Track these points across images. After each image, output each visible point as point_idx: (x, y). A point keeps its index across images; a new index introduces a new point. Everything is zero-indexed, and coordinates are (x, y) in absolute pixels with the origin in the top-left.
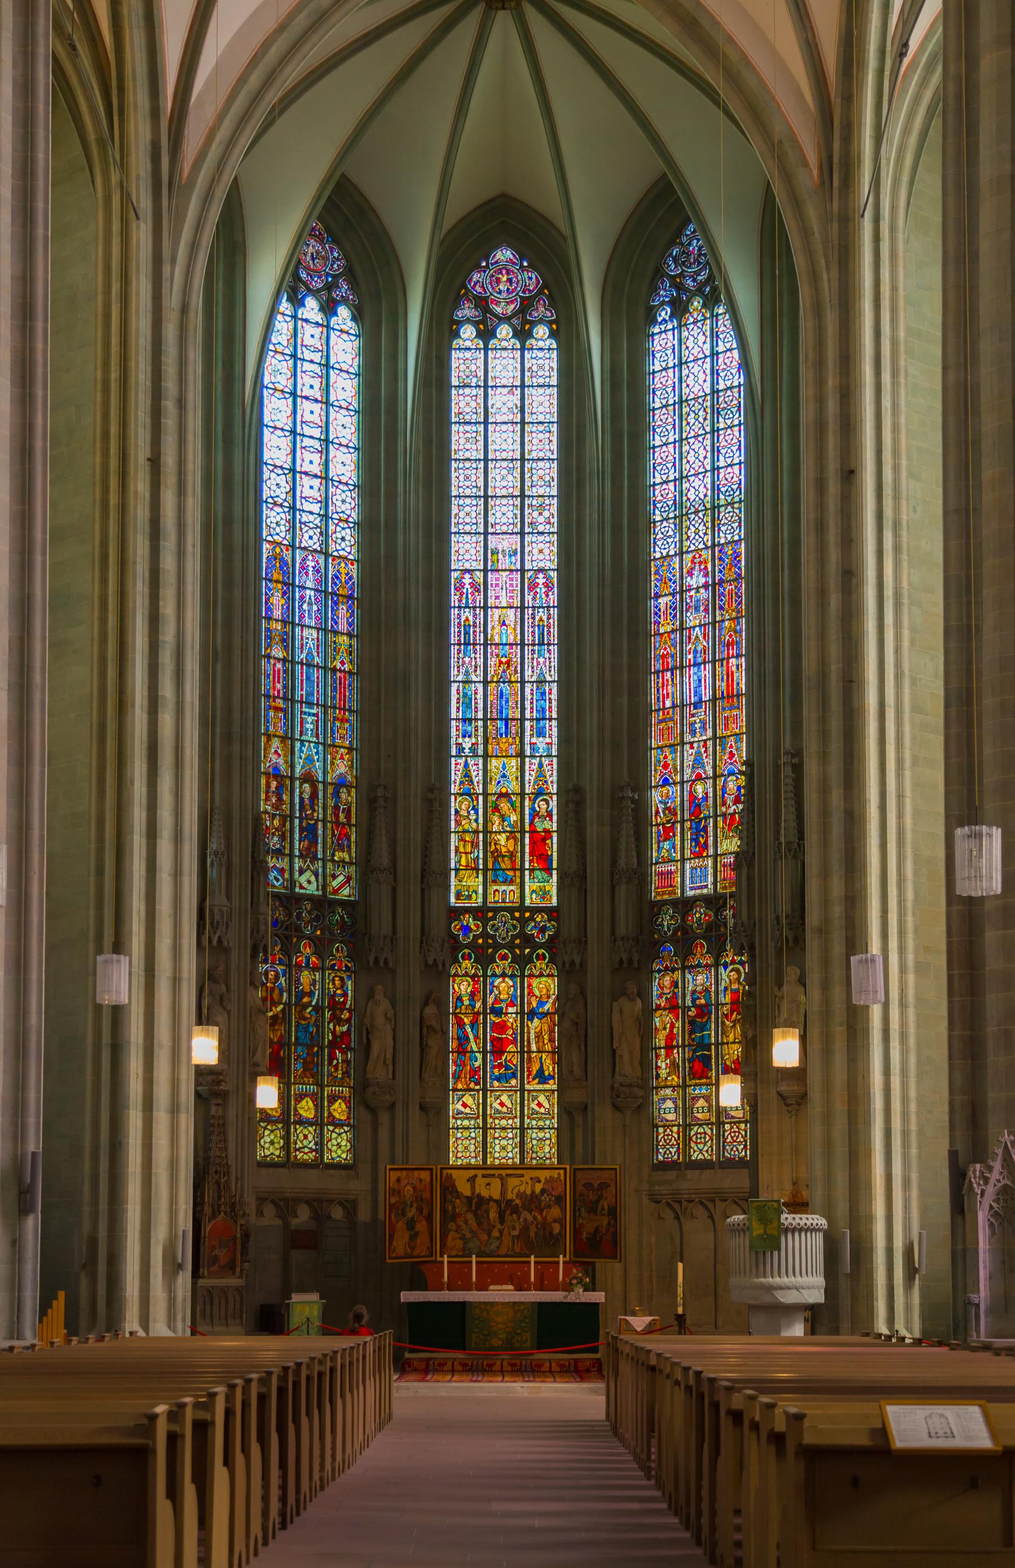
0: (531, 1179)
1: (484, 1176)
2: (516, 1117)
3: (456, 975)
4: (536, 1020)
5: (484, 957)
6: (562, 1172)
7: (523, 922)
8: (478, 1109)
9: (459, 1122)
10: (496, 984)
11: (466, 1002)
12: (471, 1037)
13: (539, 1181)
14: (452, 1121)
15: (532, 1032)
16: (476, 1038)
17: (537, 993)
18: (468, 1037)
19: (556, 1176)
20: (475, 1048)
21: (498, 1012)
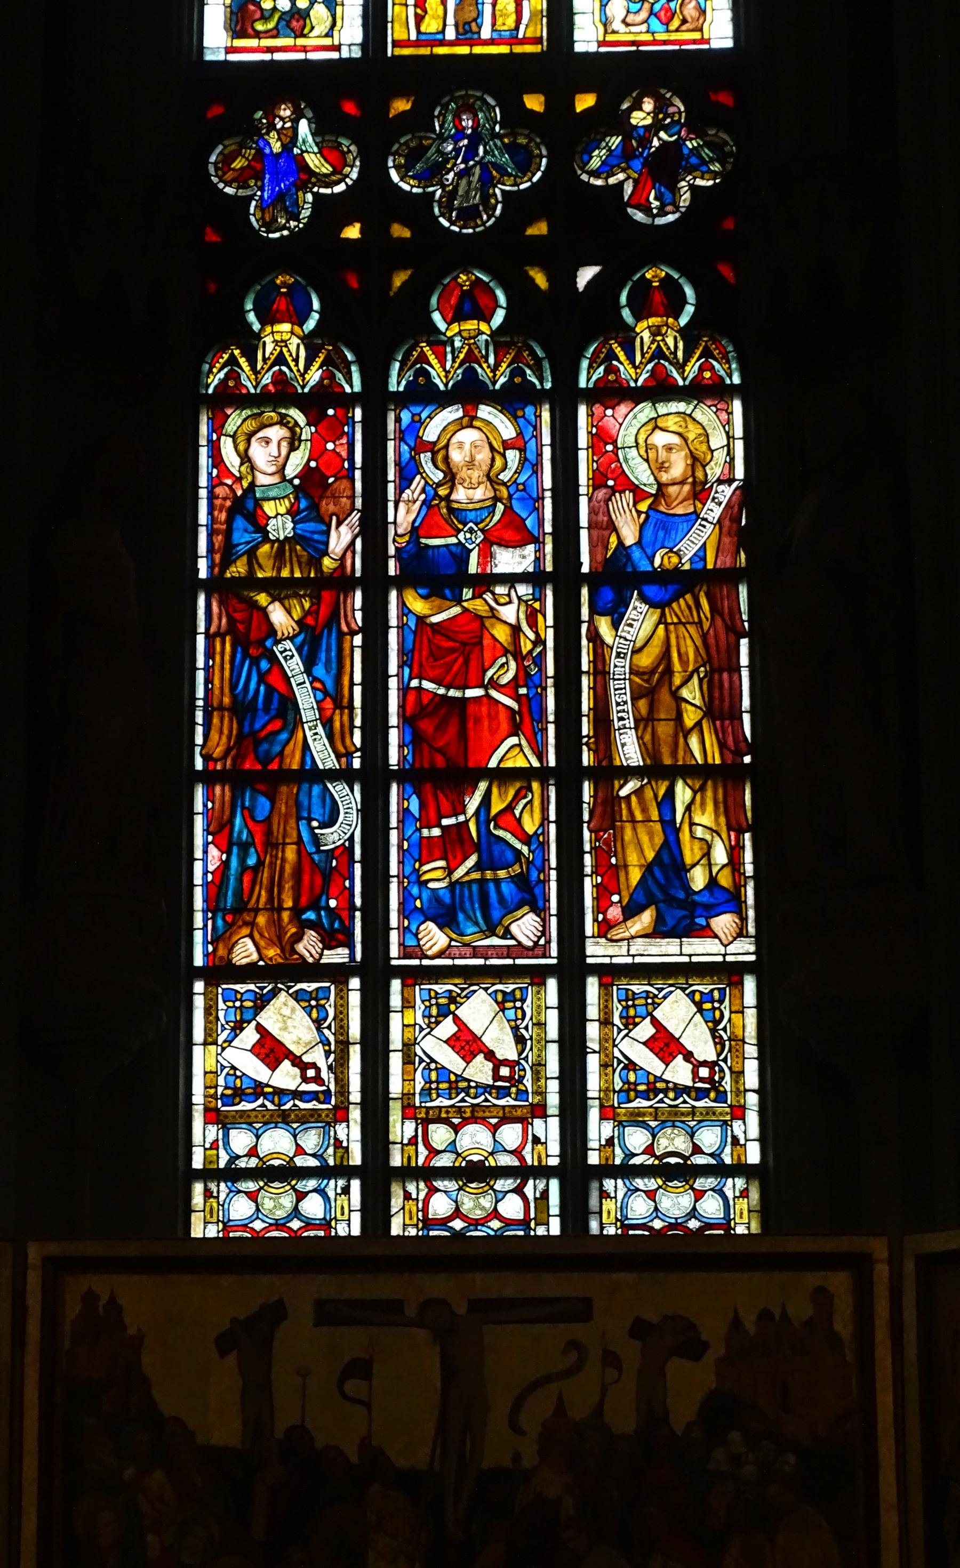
0: (639, 1329)
1: (328, 1314)
2: (540, 1111)
3: (230, 396)
4: (637, 609)
5: (373, 321)
6: (839, 1282)
7: (568, 137)
8: (340, 1066)
9: (240, 1140)
10: (431, 433)
11: (281, 527)
12: (306, 699)
13: (694, 1348)
14: (202, 1132)
15: (619, 667)
16: (333, 699)
17: (641, 474)
18: (289, 703)
19: (801, 1309)
20: (323, 756)
21: (440, 574)
